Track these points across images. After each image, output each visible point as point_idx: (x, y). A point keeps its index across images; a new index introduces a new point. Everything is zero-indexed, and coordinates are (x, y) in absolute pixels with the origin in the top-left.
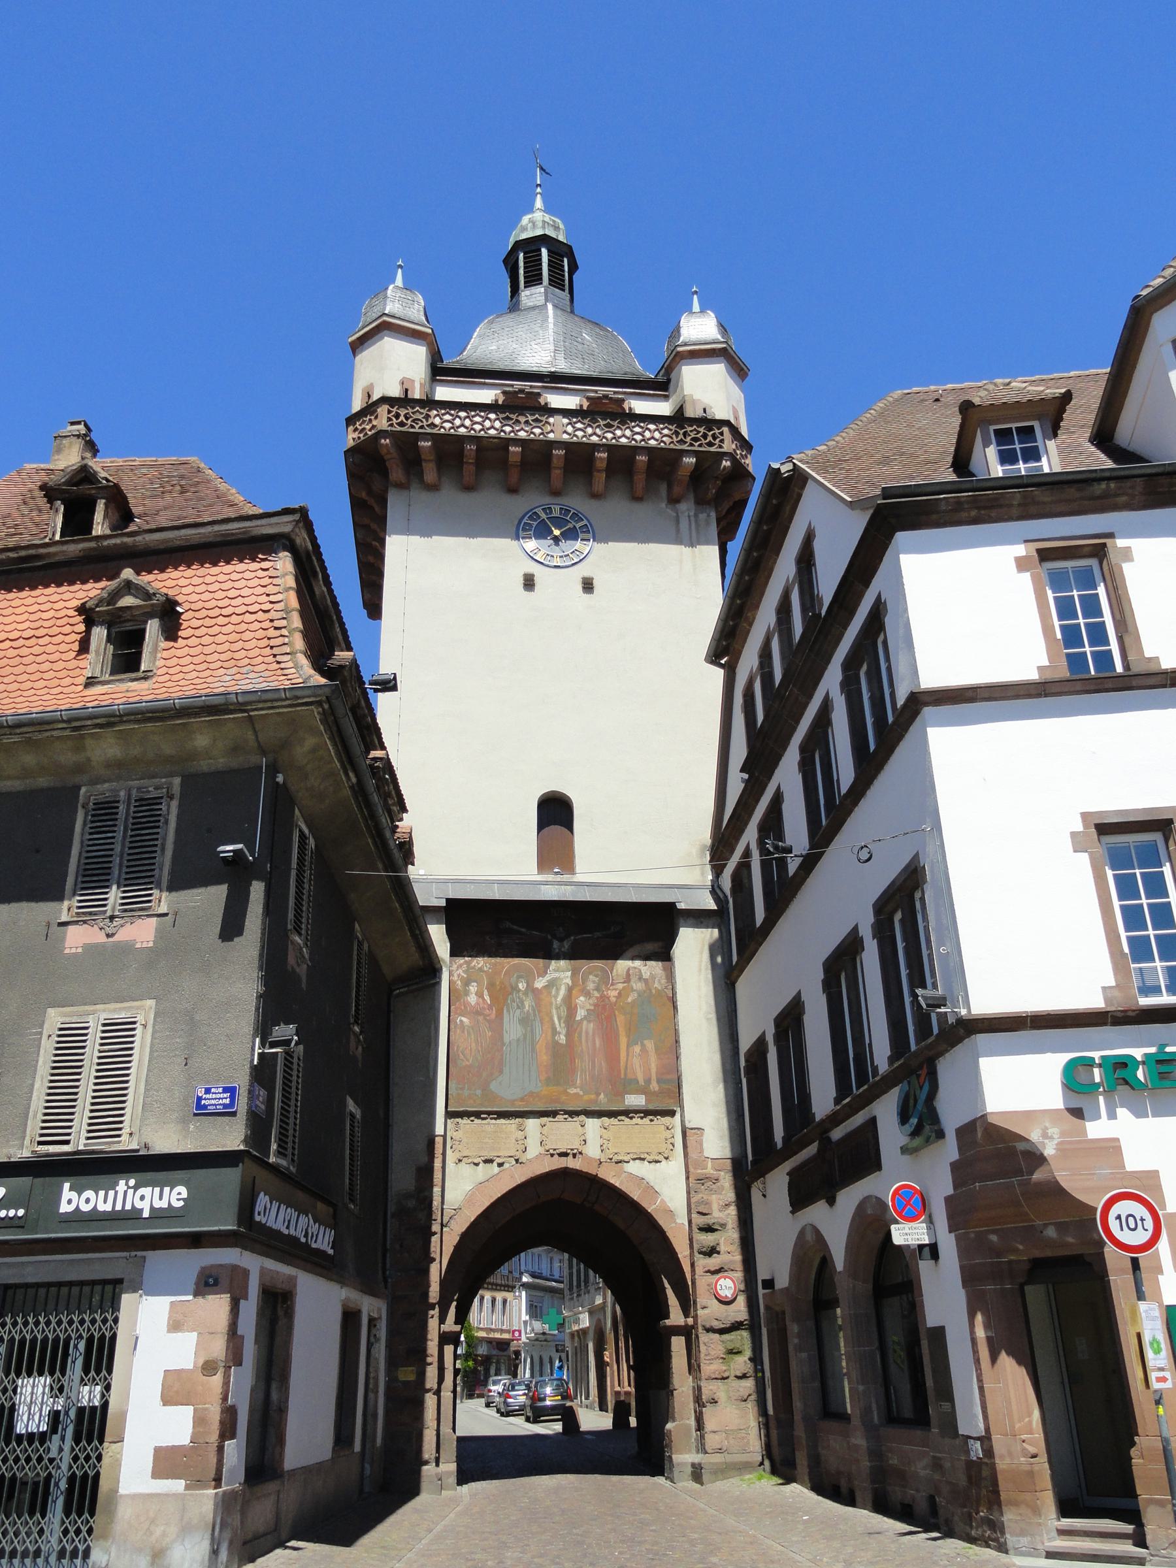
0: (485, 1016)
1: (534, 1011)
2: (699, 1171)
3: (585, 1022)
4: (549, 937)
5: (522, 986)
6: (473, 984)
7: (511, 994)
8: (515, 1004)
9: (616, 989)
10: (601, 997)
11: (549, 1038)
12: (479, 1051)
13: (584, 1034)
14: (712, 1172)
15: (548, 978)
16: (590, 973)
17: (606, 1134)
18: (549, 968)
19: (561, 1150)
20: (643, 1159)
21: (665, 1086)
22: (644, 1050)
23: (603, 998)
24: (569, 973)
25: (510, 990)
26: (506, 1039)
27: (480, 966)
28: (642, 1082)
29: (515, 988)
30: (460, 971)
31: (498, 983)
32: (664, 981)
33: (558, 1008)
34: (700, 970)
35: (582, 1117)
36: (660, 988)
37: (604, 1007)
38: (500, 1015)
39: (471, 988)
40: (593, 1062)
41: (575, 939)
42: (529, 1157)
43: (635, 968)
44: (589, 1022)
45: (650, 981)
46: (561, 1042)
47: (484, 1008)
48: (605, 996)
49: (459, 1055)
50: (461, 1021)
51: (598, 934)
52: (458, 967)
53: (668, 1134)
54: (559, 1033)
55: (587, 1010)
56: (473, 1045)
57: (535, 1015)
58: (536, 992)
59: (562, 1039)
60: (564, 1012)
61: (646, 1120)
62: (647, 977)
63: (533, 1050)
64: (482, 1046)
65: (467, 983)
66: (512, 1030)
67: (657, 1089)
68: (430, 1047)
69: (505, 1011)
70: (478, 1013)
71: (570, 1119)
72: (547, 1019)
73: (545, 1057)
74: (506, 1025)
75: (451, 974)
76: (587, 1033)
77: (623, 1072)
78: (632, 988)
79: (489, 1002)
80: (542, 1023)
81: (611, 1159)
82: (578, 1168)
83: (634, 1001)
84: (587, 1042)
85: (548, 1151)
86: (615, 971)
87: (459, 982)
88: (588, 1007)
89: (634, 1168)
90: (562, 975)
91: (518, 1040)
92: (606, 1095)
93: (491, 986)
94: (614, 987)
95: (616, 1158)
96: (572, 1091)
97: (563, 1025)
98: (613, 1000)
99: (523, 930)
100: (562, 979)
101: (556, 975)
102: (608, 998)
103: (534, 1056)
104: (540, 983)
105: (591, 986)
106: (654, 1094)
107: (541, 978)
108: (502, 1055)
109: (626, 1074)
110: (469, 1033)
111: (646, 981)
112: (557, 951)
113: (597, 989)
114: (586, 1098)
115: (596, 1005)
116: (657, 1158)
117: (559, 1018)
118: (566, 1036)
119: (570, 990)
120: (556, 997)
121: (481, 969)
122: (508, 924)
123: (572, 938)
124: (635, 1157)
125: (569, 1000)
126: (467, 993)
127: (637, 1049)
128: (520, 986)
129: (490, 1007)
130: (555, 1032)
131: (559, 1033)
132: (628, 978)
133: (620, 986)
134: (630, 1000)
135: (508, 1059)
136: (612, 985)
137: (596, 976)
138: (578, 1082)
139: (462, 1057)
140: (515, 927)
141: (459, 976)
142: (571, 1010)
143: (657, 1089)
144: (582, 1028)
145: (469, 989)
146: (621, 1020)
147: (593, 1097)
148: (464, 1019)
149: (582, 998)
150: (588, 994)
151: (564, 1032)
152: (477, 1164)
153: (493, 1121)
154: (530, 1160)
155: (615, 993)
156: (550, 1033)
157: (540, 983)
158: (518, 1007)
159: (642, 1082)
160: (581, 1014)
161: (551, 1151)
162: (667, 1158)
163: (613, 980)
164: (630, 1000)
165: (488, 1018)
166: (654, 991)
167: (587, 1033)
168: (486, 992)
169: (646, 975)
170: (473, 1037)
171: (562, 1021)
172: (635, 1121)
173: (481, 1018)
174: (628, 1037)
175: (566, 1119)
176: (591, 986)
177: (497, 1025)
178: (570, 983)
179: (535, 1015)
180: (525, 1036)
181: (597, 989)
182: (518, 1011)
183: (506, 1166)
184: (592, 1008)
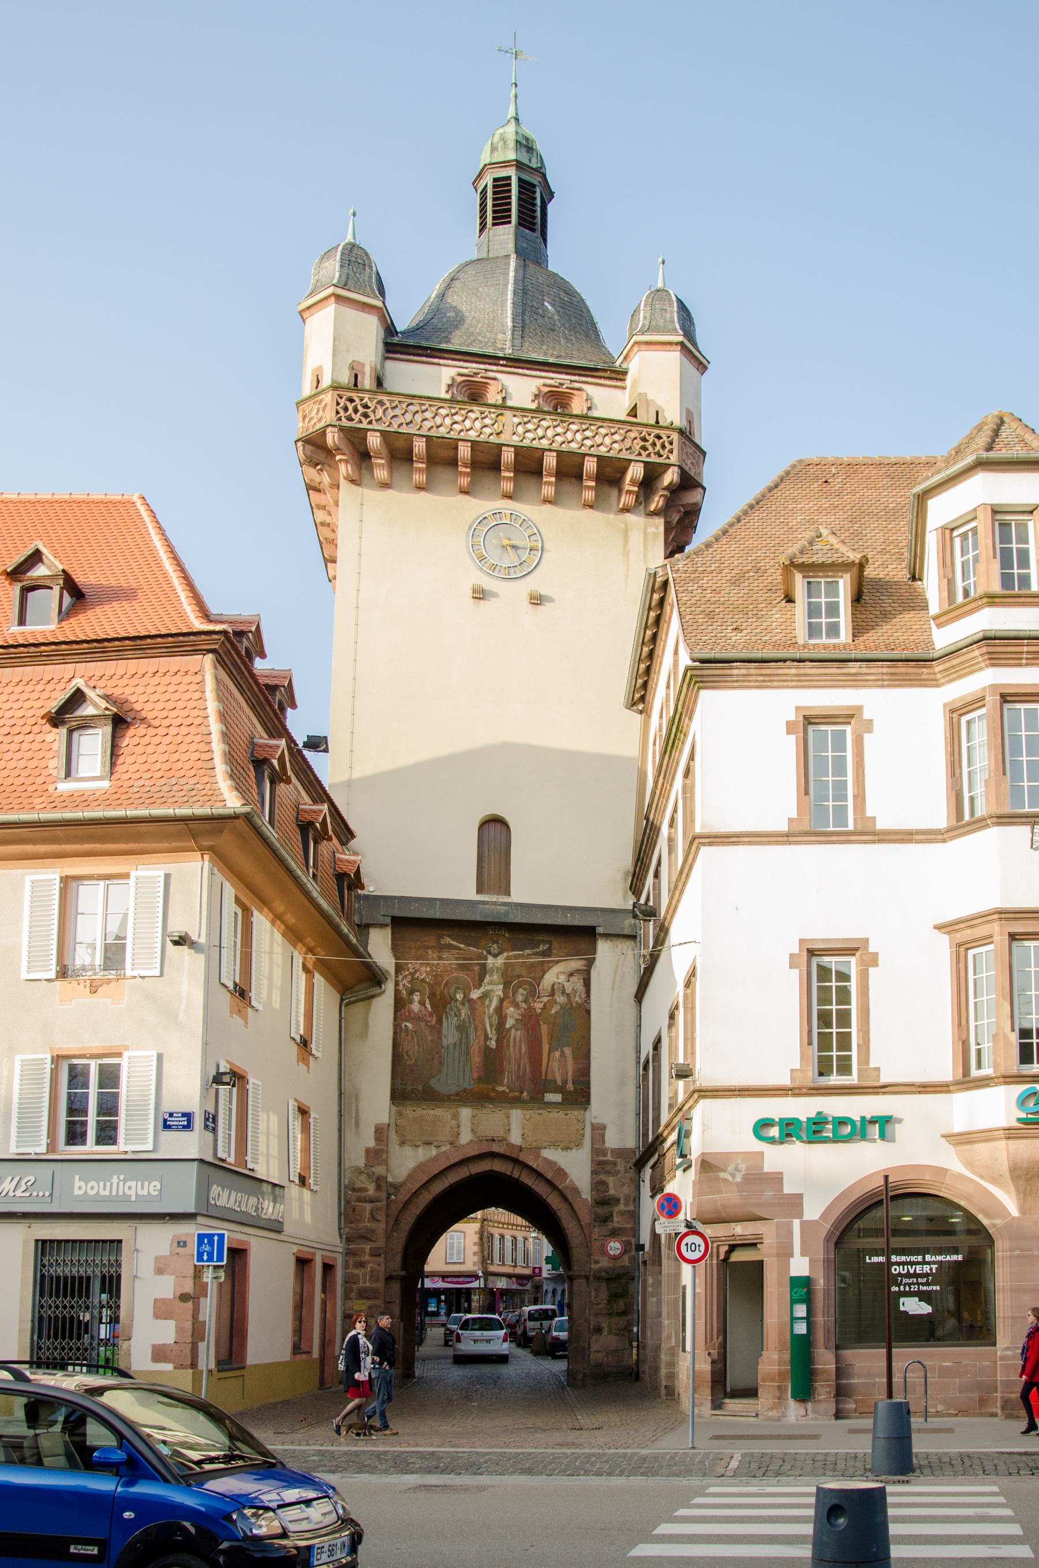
0: (427, 1022)
1: (469, 1018)
3: (513, 1030)
4: (485, 953)
5: (459, 996)
7: (450, 1003)
11: (482, 1043)
13: (512, 1040)
15: (482, 989)
16: (519, 987)
22: (563, 1054)
23: (530, 1009)
24: (501, 987)
26: (445, 1042)
28: (559, 1082)
29: (453, 999)
30: (405, 982)
32: (583, 996)
33: (490, 1017)
37: (531, 1017)
38: (440, 1021)
39: (415, 997)
40: (519, 1066)
44: (516, 1030)
47: (425, 1015)
49: (403, 1056)
50: (406, 1026)
54: (491, 1039)
56: (416, 1047)
57: (470, 1023)
58: (470, 1001)
59: (493, 1044)
60: (495, 1021)
63: (468, 1053)
65: (411, 992)
66: (450, 1035)
70: (419, 1019)
72: (480, 1026)
74: (445, 1031)
75: (397, 983)
76: (515, 1039)
77: (544, 1074)
78: (556, 1001)
80: (476, 1030)
83: (556, 1013)
84: (514, 1046)
88: (517, 1017)
89: (548, 1154)
90: (495, 988)
91: (455, 1044)
92: (528, 1093)
93: (432, 996)
94: (541, 1000)
96: (500, 1089)
97: (494, 1032)
98: (539, 1011)
99: (462, 946)
101: (490, 987)
102: (534, 1009)
104: (475, 995)
105: (520, 998)
106: (570, 1092)
108: (440, 1057)
109: (546, 1076)
111: (568, 995)
112: (491, 965)
113: (526, 1001)
114: (511, 1095)
115: (523, 1015)
117: (491, 1026)
118: (496, 1042)
119: (501, 1001)
120: (489, 1007)
121: (423, 980)
122: (447, 940)
123: (505, 954)
125: (499, 1010)
126: (411, 1002)
127: (557, 1054)
130: (487, 1038)
131: (491, 1039)
132: (552, 994)
133: (545, 999)
134: (553, 1011)
136: (538, 998)
137: (525, 989)
138: (506, 1081)
139: (406, 1057)
140: (455, 943)
141: (404, 985)
142: (502, 1019)
144: (510, 1036)
146: (544, 1029)
147: (517, 1094)
148: (408, 1024)
149: (512, 1009)
150: (516, 1005)
151: (495, 1038)
153: (432, 1112)
155: (541, 1005)
156: (482, 1038)
157: (475, 995)
158: (456, 1015)
159: (559, 1082)
160: (510, 1023)
166: (574, 1005)
167: (515, 1039)
168: (427, 1001)
173: (422, 1024)
176: (520, 998)
177: (437, 1029)
178: (502, 996)
179: (470, 1023)
180: (461, 1041)
181: (526, 1001)
182: (456, 1018)
184: (520, 1018)
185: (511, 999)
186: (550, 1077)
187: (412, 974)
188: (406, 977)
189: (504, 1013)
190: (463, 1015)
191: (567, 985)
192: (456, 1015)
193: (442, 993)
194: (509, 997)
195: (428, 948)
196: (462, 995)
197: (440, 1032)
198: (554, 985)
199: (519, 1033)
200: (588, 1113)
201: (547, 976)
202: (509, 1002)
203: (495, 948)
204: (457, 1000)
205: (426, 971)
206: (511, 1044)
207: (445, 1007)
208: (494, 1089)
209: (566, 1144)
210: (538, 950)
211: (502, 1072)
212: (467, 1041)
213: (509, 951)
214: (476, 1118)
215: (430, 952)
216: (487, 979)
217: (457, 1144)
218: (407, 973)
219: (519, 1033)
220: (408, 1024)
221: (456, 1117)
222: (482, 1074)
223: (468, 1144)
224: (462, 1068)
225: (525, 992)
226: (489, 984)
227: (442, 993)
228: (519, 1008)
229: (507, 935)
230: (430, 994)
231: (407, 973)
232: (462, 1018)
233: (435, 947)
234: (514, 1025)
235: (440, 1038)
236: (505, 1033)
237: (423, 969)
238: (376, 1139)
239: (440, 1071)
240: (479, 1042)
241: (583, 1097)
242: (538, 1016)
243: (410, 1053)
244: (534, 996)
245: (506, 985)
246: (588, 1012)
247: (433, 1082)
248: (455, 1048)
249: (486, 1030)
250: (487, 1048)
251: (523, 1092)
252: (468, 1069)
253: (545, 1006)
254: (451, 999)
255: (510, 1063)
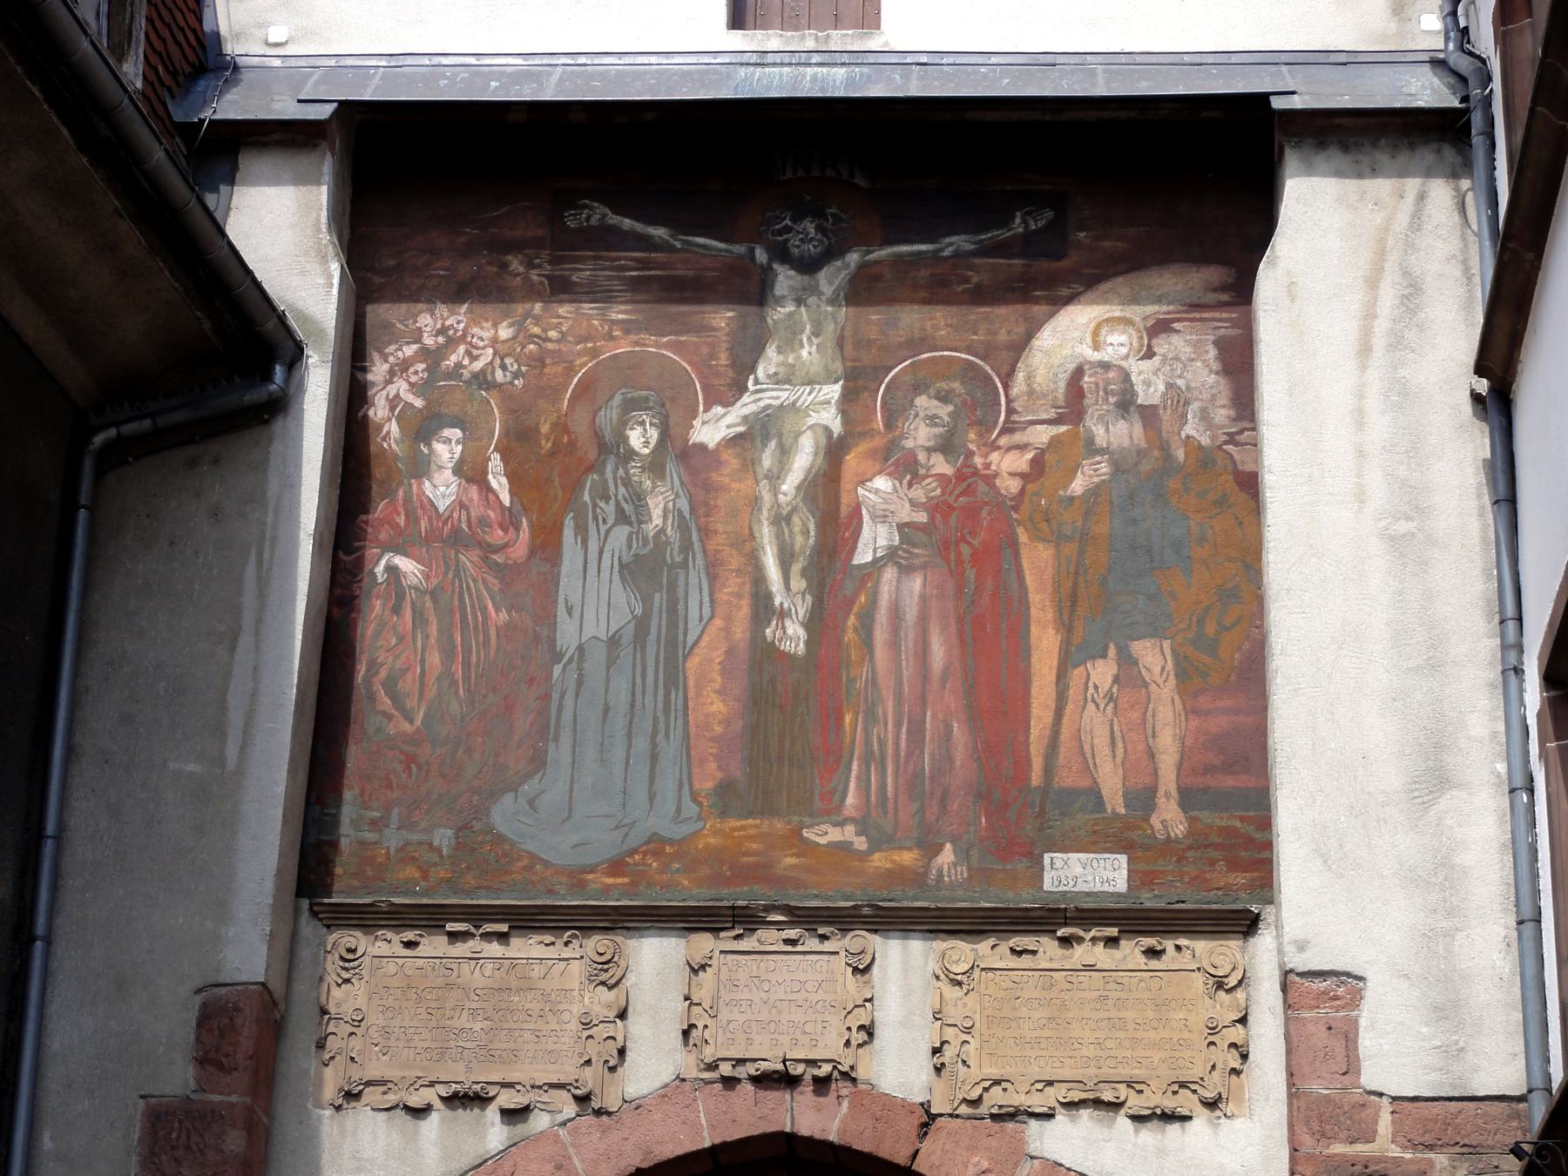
0: (489, 549)
1: (683, 528)
2: (1338, 1148)
3: (889, 574)
4: (761, 255)
5: (640, 438)
6: (447, 432)
8: (610, 509)
9: (1022, 447)
10: (960, 476)
11: (740, 631)
12: (454, 683)
14: (1395, 1152)
15: (747, 406)
16: (918, 388)
17: (960, 1005)
18: (753, 369)
19: (764, 1066)
20: (1115, 1106)
21: (1208, 817)
23: (967, 477)
24: (834, 391)
25: (592, 455)
26: (567, 635)
27: (478, 365)
28: (1115, 801)
30: (400, 387)
31: (545, 429)
32: (1222, 415)
33: (781, 520)
34: (1365, 350)
35: (861, 939)
36: (1205, 440)
37: (972, 513)
38: (547, 544)
39: (439, 447)
40: (917, 731)
41: (862, 266)
42: (632, 1091)
43: (1105, 366)
44: (906, 570)
45: (1166, 416)
46: (786, 646)
47: (484, 522)
48: (976, 473)
50: (392, 570)
51: (958, 242)
52: (392, 373)
53: (1224, 1008)
54: (783, 614)
55: (901, 527)
56: (435, 659)
57: (686, 547)
58: (695, 460)
59: (793, 636)
61: (1131, 951)
62: (1155, 400)
63: (673, 676)
64: (466, 664)
65: (423, 428)
67: (1179, 830)
68: (233, 649)
69: (568, 533)
70: (457, 539)
71: (813, 944)
72: (735, 561)
73: (717, 706)
74: (569, 585)
76: (896, 613)
77: (1037, 762)
78: (1090, 441)
79: (506, 498)
80: (713, 578)
81: (975, 1103)
82: (832, 1137)
83: (1094, 492)
84: (894, 643)
85: (712, 1067)
86: (1020, 376)
87: (394, 428)
88: (905, 514)
90: (805, 396)
91: (614, 642)
92: (963, 853)
94: (1018, 438)
95: (996, 1098)
96: (825, 835)
97: (798, 584)
99: (659, 232)
100: (805, 412)
101: (784, 395)
102: (990, 479)
103: (676, 699)
105: (919, 435)
106: (1168, 846)
107: (719, 410)
108: (546, 697)
109: (1048, 770)
110: (419, 618)
111: (1149, 415)
113: (946, 446)
114: (879, 861)
115: (937, 508)
116: (1169, 1103)
118: (807, 626)
119: (834, 451)
120: (775, 478)
121: (482, 380)
122: (599, 214)
123: (853, 258)
124: (1076, 1096)
126: (421, 467)
128: (635, 438)
129: (509, 520)
130: (763, 609)
131: (783, 614)
132: (1073, 405)
133: (1042, 435)
134: (1078, 486)
135: (567, 716)
136: (1008, 429)
137: (943, 398)
138: (850, 800)
139: (385, 702)
140: (627, 223)
141: (394, 402)
143: (1179, 830)
145: (431, 451)
147: (908, 858)
148: (405, 564)
149: (882, 483)
150: (907, 468)
151: (802, 608)
152: (420, 1112)
153: (495, 949)
154: (636, 1105)
155: (1021, 461)
156: (744, 609)
158: (622, 518)
159: (1115, 801)
160: (873, 541)
161: (726, 1069)
162: (1212, 1105)
163: (1011, 411)
164: (1078, 486)
165: (499, 558)
166: (1180, 454)
167: (896, 613)
168: (495, 463)
169: (1149, 383)
170: (433, 629)
171: (796, 568)
172: (1081, 954)
173: (468, 560)
174: (1066, 627)
175: (793, 942)
176: (919, 435)
178: (837, 426)
179: (686, 547)
180: (641, 626)
181: (946, 446)
182: (621, 533)
183: (540, 1122)
184: (922, 517)
185: (877, 442)
186: (1068, 778)
187: (432, 357)
188: (404, 366)
189: (845, 499)
190: (657, 520)
191: (1140, 371)
192: (622, 518)
193: (561, 427)
194: (865, 434)
195: (513, 247)
196: (654, 434)
197: (548, 587)
198: (1079, 372)
199: (916, 583)
200: (1264, 941)
201: (1046, 338)
202: (872, 454)
203: (806, 235)
204: (631, 454)
205: (494, 341)
206: (881, 635)
207: (575, 487)
208: (795, 839)
209: (1155, 1098)
210: (1002, 234)
211: (835, 759)
212: (673, 624)
213: (865, 241)
214: (706, 977)
215: (516, 265)
216: (770, 361)
217: (612, 1103)
218: (409, 350)
219: (916, 583)
220: (405, 564)
221: (607, 974)
222: (738, 771)
223: (664, 1094)
224: (641, 744)
225: (944, 411)
226: (778, 380)
227: (561, 427)
228: (916, 478)
229: (860, 181)
230: (506, 432)
231: (409, 350)
232: (650, 529)
233: (537, 244)
234: (892, 554)
235: (547, 619)
236: (849, 587)
237: (482, 333)
238: (203, 1061)
239: (538, 762)
240: (727, 631)
241: (1235, 865)
242: (1005, 508)
243: (407, 684)
244: (985, 425)
245: (857, 384)
246: (1250, 484)
247: (504, 815)
248: (611, 661)
249: (759, 579)
250: (765, 655)
251: (937, 849)
252: (670, 750)
253: (1038, 464)
254: (604, 448)
255: (871, 717)
